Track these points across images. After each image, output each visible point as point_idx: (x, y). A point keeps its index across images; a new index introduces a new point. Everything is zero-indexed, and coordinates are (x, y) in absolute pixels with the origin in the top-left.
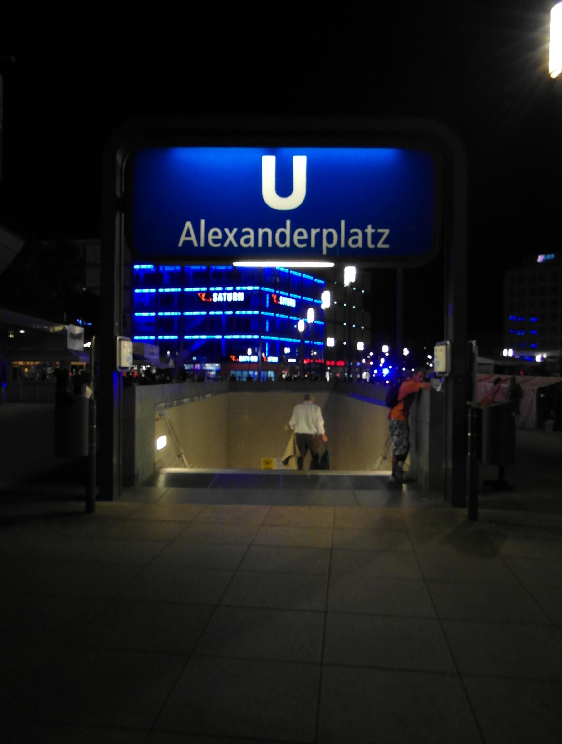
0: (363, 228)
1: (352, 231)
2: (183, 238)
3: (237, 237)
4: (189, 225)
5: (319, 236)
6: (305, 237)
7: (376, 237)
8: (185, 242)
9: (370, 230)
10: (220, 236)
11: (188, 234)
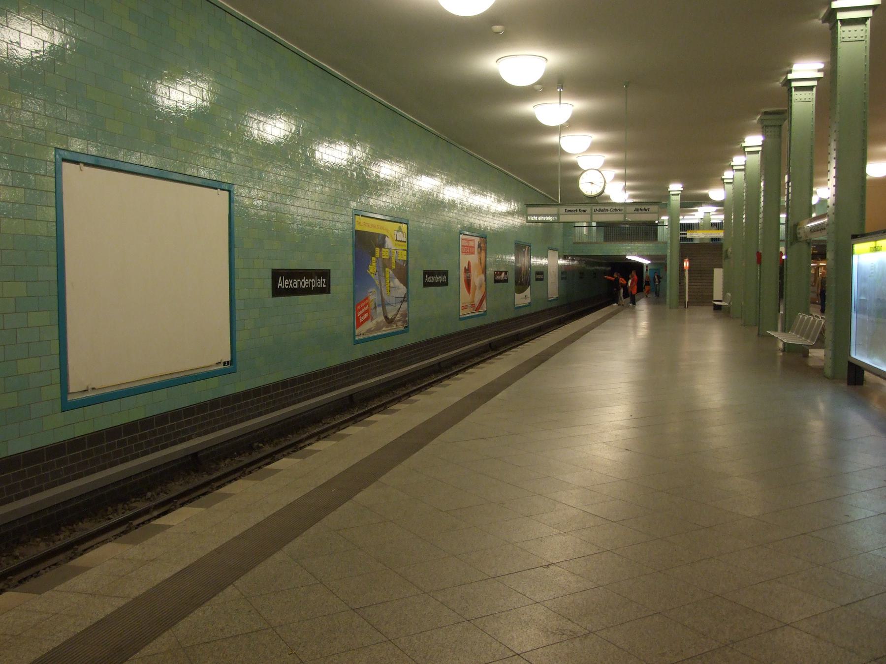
0: (320, 279)
1: (318, 280)
2: (279, 285)
3: (293, 282)
5: (311, 283)
6: (308, 283)
7: (323, 282)
8: (280, 286)
9: (321, 280)
10: (288, 283)
11: (280, 283)
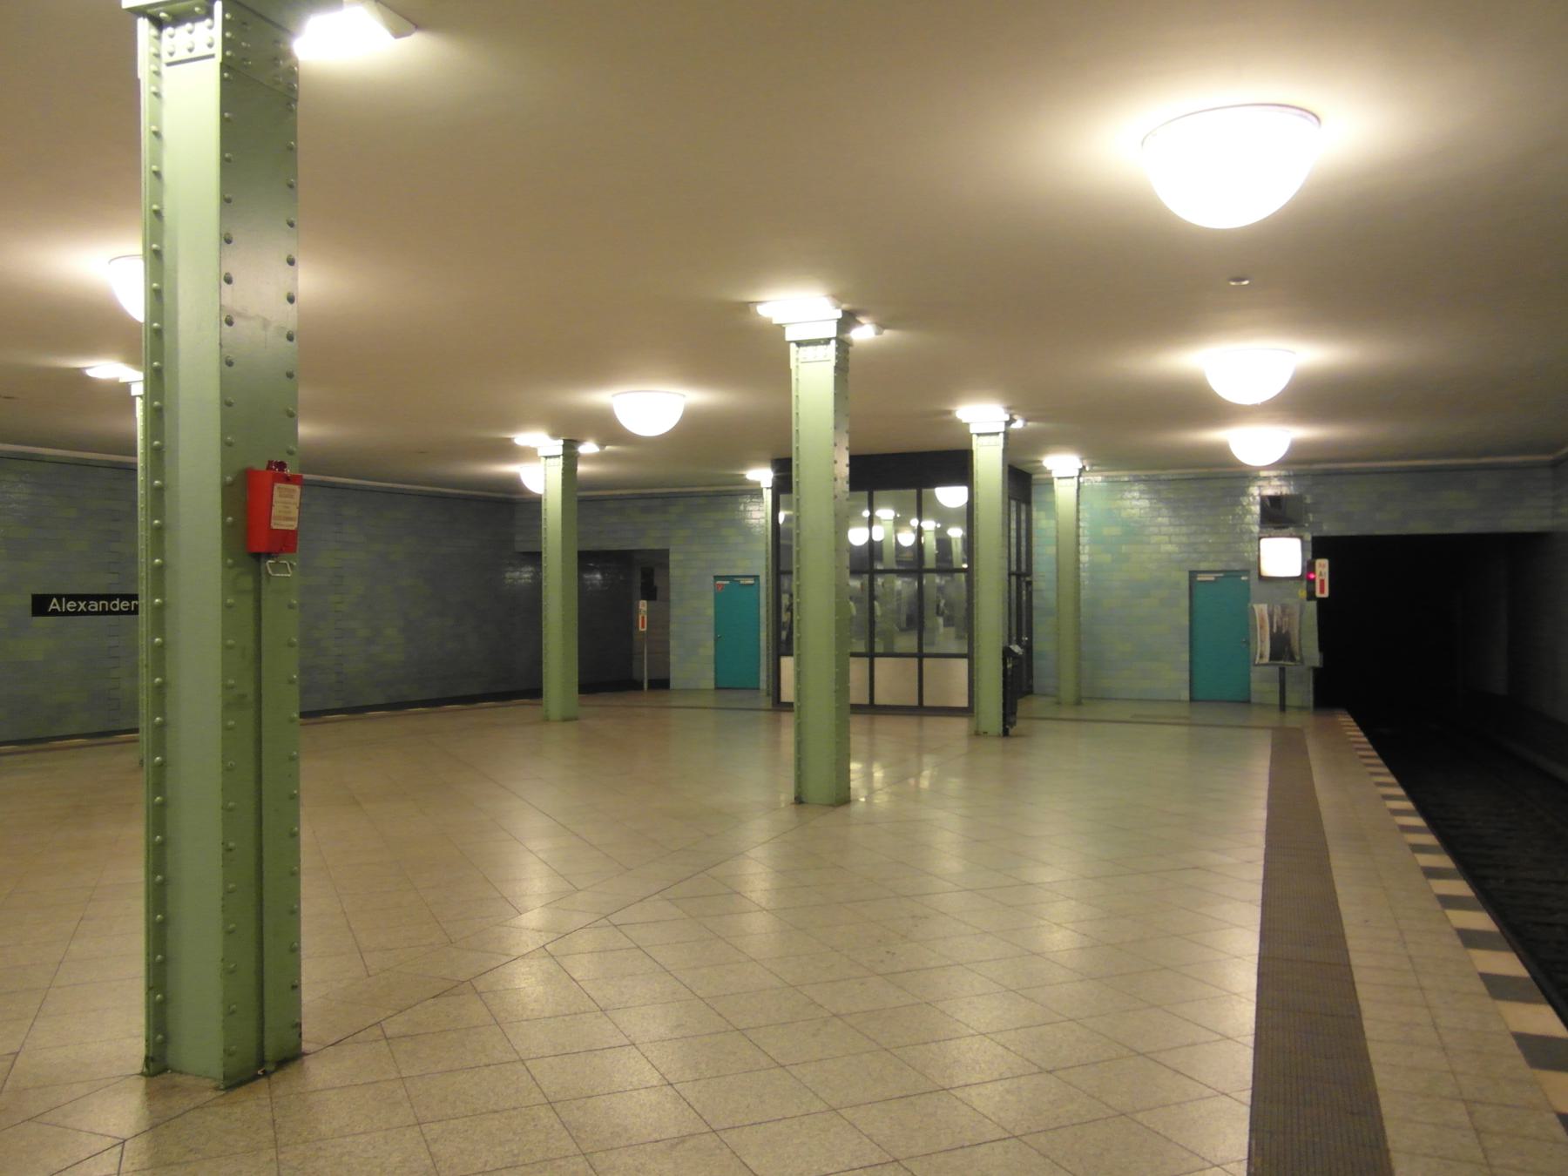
2: (52, 607)
3: (86, 606)
4: (55, 600)
10: (75, 605)
11: (55, 605)
